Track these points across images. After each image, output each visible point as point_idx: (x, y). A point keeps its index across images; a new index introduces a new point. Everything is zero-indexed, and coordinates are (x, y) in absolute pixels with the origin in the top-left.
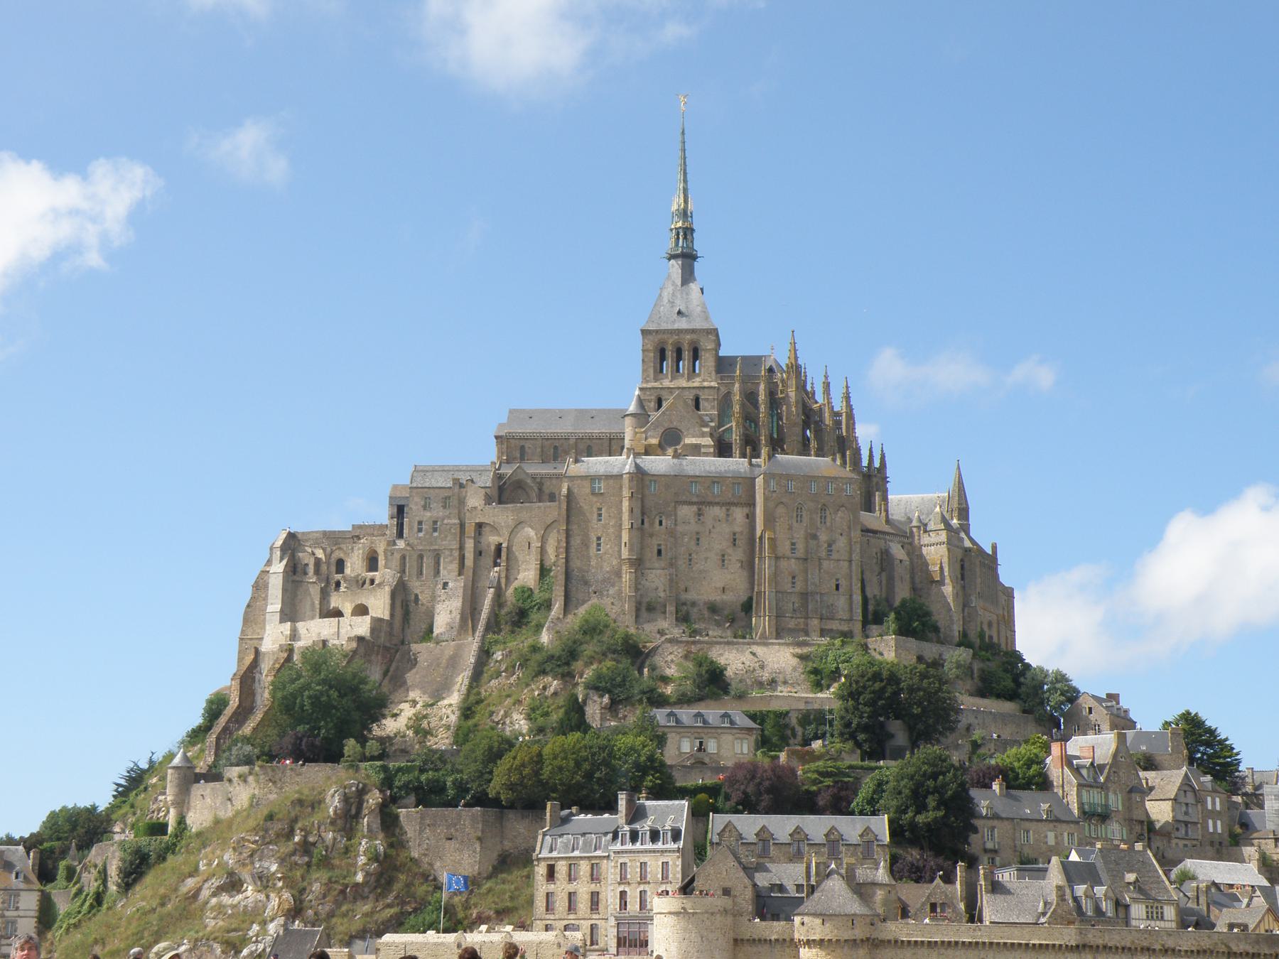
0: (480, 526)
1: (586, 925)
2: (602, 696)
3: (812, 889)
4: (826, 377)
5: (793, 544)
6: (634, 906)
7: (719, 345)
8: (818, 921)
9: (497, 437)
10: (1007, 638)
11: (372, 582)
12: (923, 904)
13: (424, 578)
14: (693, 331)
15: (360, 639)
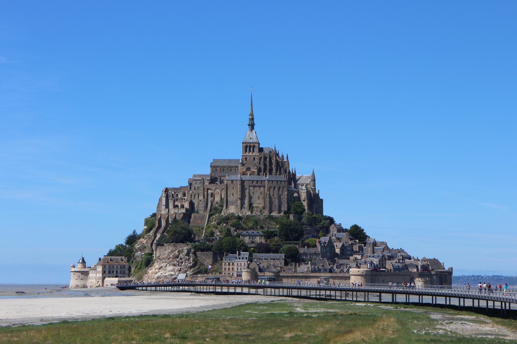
0: (208, 189)
1: (231, 273)
2: (234, 228)
3: (268, 267)
4: (282, 154)
5: (273, 194)
6: (239, 270)
7: (259, 144)
8: (269, 273)
9: (211, 167)
10: (320, 210)
11: (185, 199)
12: (287, 270)
13: (196, 199)
14: (254, 143)
15: (184, 213)
